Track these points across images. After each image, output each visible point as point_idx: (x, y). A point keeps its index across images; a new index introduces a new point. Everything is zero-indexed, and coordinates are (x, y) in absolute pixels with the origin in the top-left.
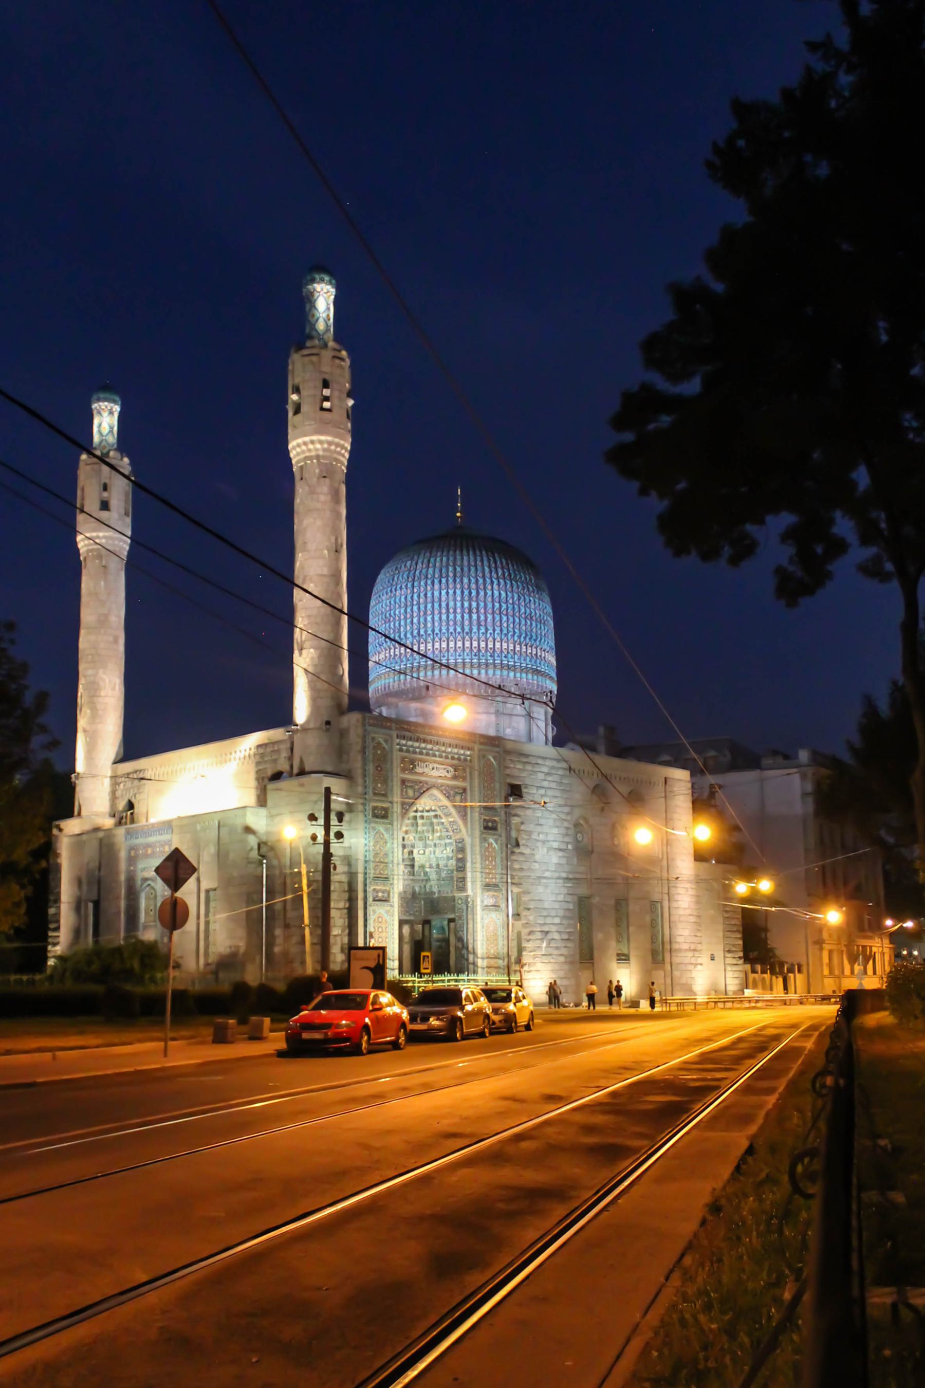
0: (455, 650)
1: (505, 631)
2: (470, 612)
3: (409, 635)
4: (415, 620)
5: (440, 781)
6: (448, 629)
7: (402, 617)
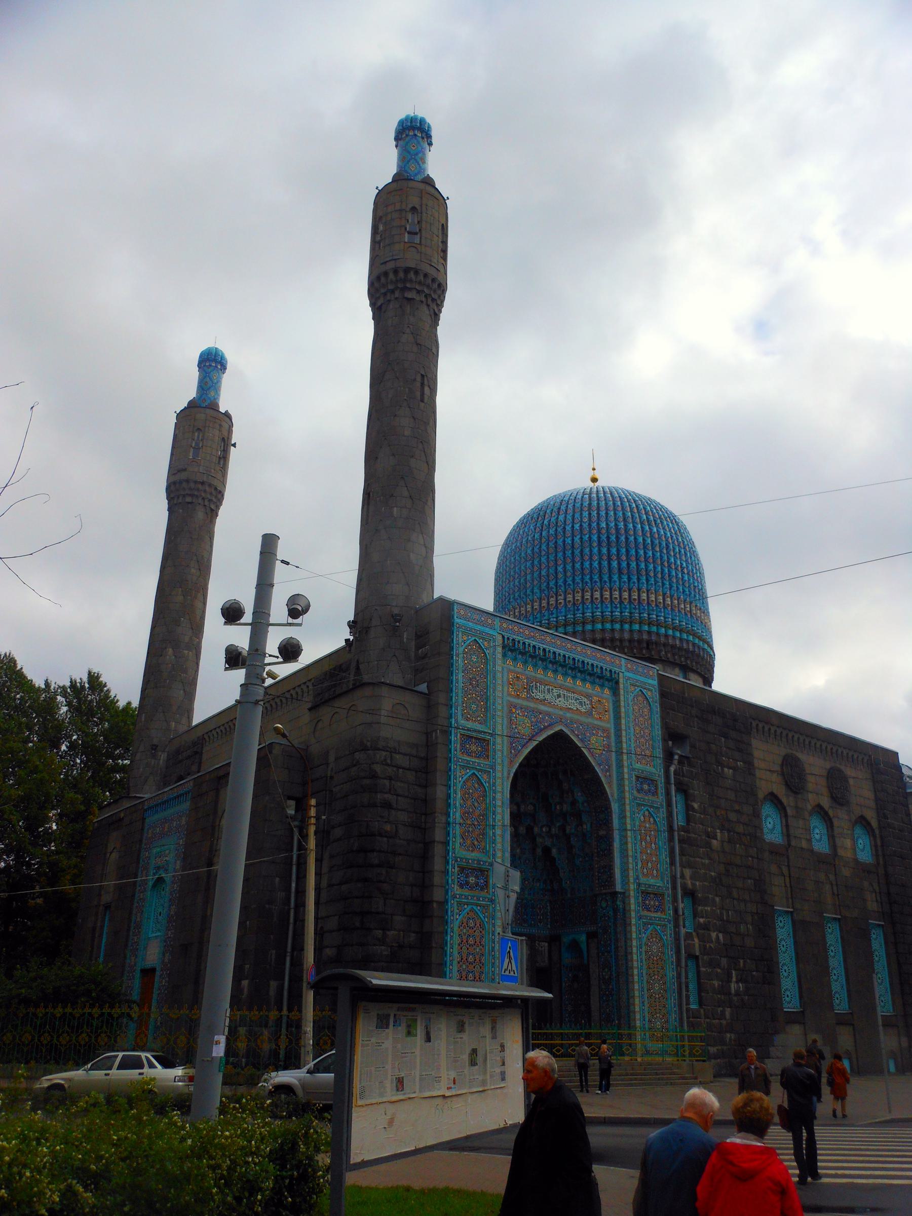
1: (652, 581)
2: (609, 560)
3: (536, 590)
4: (543, 573)
5: (568, 715)
7: (529, 571)
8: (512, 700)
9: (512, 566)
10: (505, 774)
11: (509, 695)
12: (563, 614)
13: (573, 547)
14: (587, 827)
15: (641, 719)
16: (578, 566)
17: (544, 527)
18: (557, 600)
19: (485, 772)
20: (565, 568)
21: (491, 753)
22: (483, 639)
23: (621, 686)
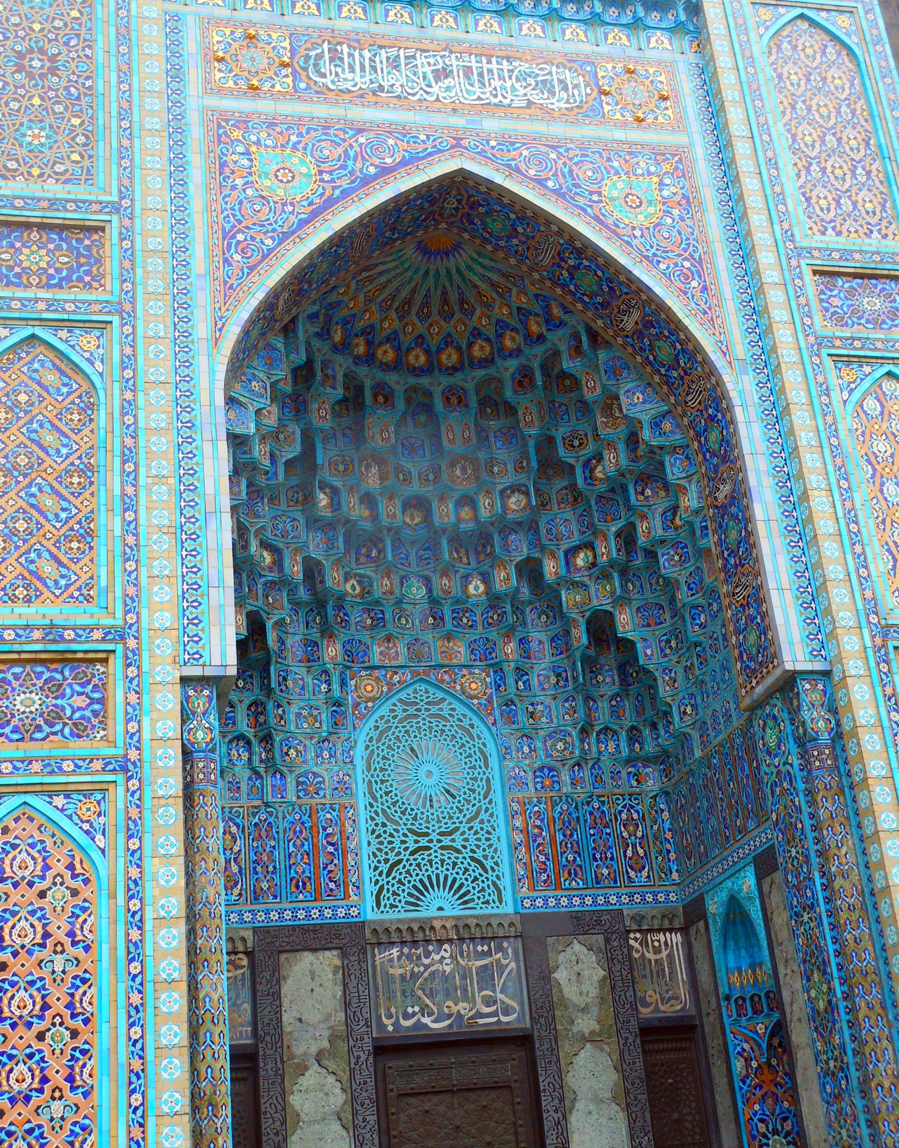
5: (491, 125)
8: (228, 104)
10: (202, 329)
11: (212, 89)
14: (691, 500)
15: (820, 100)
19: (88, 325)
21: (112, 266)
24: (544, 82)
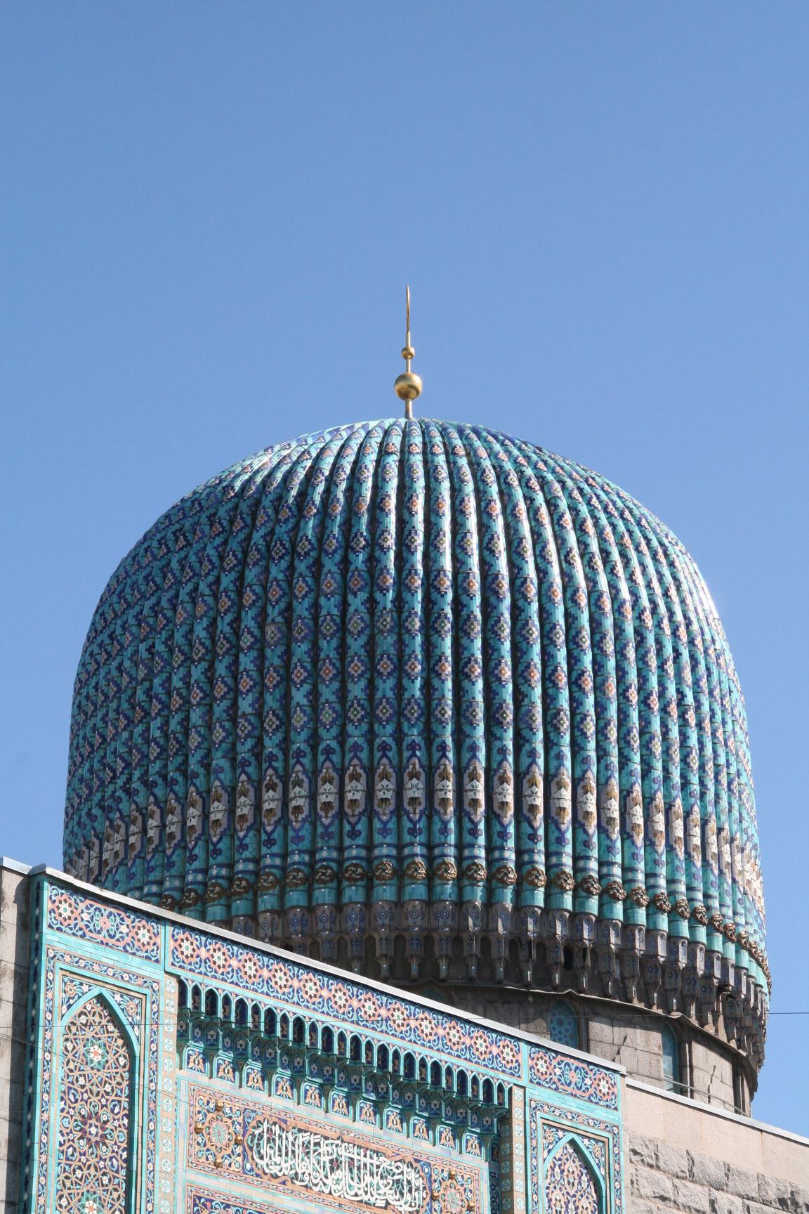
0: (399, 811)
3: (219, 760)
4: (245, 705)
6: (371, 735)
7: (196, 696)
9: (142, 673)
11: (193, 1164)
12: (305, 845)
13: (343, 628)
16: (357, 690)
17: (254, 555)
18: (285, 801)
20: (314, 694)
22: (124, 991)
23: (517, 1129)
24: (398, 1181)
